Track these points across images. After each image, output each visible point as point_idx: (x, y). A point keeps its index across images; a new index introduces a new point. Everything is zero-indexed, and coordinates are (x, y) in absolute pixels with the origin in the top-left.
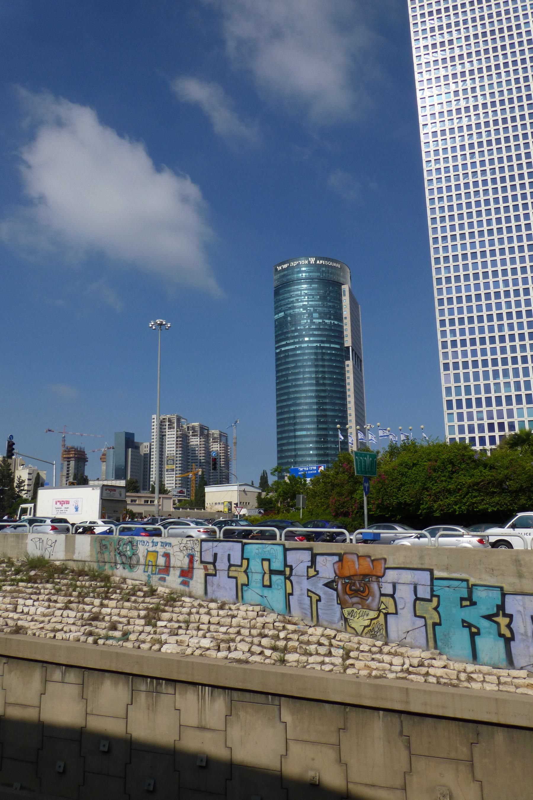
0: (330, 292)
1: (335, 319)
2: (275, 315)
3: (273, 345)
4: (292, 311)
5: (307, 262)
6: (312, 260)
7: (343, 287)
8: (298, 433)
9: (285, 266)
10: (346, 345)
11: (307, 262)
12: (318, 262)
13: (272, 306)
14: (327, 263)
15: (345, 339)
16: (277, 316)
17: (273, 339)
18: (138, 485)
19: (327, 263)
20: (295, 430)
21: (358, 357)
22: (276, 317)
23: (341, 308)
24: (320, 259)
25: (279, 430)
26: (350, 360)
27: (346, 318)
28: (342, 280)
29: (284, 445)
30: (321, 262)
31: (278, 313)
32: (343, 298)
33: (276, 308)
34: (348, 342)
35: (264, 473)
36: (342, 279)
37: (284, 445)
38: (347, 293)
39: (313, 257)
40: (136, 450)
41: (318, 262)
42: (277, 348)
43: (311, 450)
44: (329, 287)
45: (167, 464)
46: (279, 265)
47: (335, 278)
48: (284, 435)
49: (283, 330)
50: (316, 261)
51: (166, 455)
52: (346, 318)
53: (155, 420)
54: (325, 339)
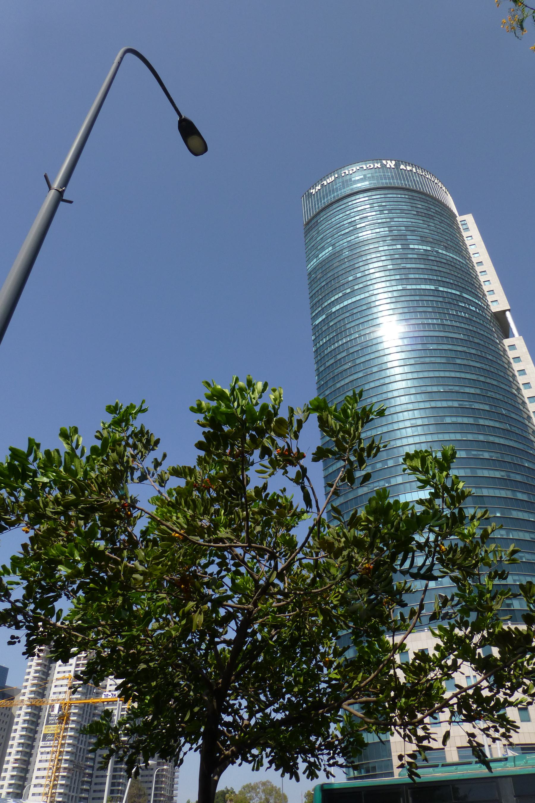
4: (353, 237)
6: (391, 164)
10: (495, 308)
12: (402, 167)
14: (419, 171)
15: (490, 298)
24: (406, 164)
30: (409, 168)
42: (314, 318)
45: (47, 723)
50: (397, 166)
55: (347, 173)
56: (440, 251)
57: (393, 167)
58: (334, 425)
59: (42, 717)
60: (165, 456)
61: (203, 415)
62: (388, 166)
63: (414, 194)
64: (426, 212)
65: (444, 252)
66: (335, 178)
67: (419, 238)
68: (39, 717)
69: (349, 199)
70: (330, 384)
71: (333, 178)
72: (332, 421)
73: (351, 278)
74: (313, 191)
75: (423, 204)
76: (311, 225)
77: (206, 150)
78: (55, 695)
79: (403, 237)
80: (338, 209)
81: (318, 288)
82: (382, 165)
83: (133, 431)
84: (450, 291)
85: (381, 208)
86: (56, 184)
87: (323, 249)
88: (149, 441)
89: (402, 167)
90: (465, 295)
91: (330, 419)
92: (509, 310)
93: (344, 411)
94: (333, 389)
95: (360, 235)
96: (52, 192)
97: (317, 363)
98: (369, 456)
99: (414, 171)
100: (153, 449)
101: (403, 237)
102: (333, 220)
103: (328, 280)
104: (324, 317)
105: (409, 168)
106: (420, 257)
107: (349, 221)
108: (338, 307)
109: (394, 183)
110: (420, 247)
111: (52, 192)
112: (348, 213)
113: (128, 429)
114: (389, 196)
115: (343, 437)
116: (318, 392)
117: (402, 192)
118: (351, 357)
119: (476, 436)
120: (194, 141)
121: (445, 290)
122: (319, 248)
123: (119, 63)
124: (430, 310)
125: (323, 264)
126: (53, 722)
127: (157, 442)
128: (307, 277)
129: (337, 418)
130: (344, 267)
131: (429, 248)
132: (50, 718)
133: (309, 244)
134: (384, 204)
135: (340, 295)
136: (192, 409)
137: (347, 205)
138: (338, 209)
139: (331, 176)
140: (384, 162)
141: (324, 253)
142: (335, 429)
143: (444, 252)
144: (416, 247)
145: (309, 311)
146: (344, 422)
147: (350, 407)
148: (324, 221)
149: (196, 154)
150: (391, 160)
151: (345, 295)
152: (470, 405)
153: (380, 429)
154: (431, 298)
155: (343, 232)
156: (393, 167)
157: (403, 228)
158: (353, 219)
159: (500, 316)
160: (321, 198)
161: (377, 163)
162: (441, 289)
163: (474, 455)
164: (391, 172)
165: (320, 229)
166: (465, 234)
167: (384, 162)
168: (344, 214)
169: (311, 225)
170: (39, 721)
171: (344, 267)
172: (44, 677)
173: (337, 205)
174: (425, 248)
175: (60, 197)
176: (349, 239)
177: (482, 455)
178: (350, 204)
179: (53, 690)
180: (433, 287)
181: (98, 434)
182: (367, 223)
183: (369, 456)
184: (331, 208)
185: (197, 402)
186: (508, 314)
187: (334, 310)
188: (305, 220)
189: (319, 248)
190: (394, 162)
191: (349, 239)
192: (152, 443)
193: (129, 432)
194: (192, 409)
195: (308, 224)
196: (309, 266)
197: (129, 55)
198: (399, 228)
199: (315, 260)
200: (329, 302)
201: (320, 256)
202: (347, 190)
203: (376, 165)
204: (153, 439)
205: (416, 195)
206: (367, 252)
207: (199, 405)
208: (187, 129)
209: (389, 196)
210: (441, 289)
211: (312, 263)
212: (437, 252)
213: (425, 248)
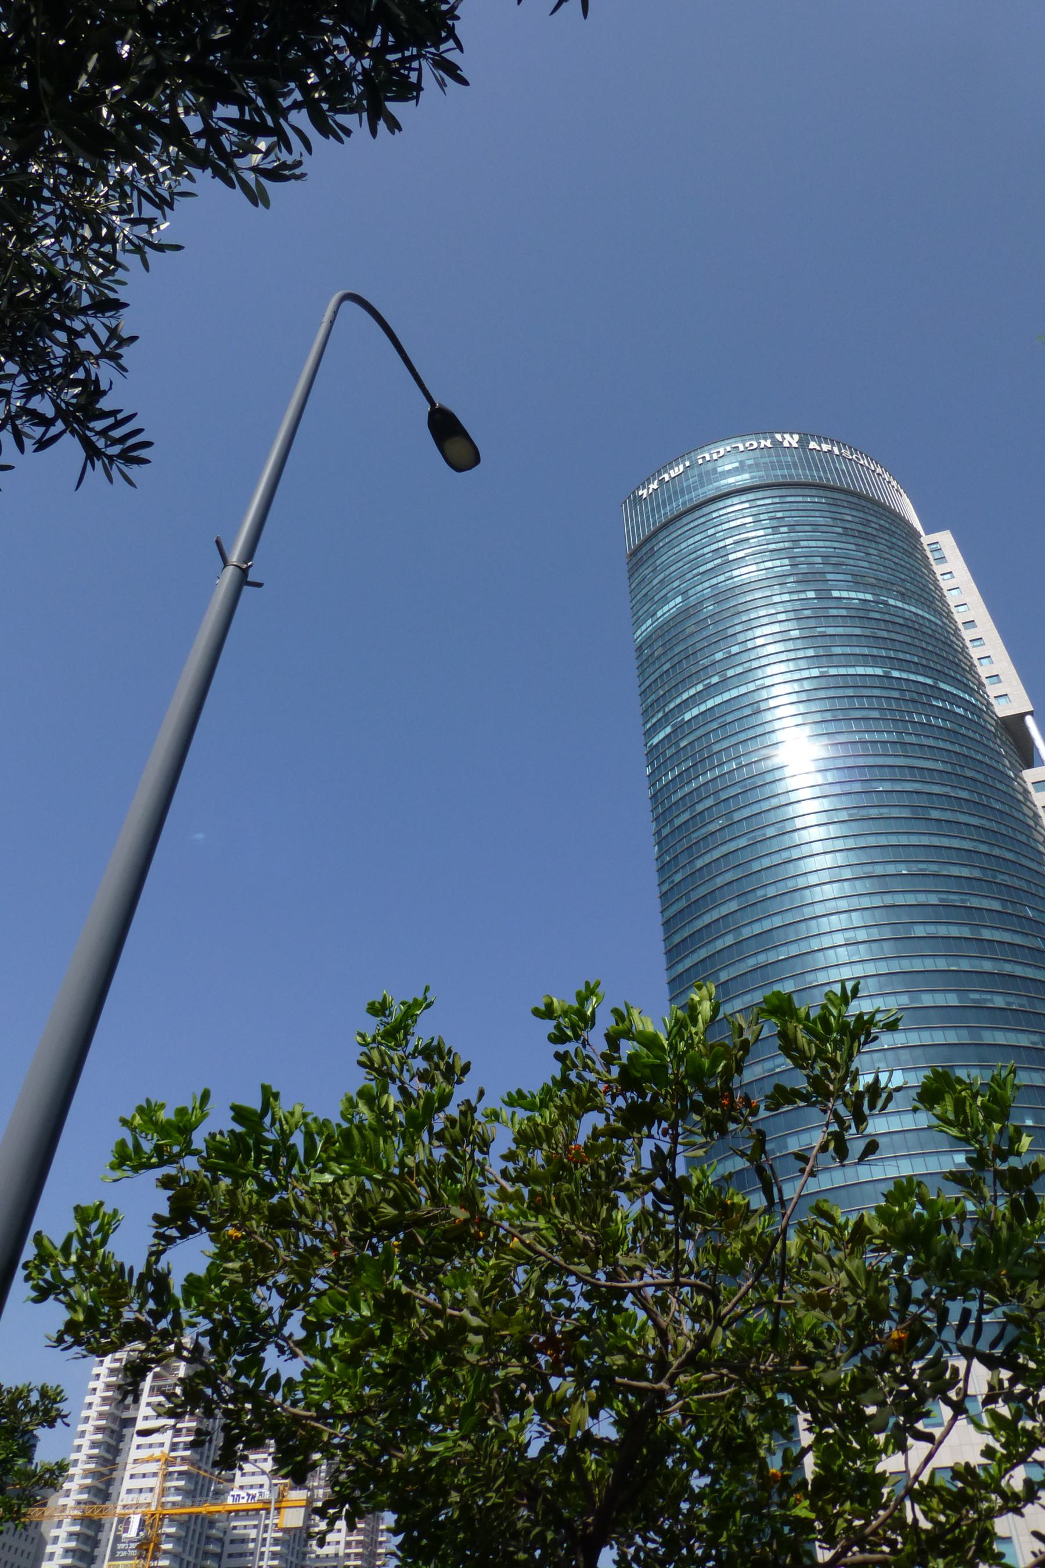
4: (722, 578)
5: (768, 443)
6: (791, 440)
10: (1003, 710)
11: (768, 443)
12: (813, 445)
14: (846, 453)
15: (992, 691)
24: (820, 439)
30: (826, 447)
42: (650, 733)
45: (113, 1557)
50: (803, 443)
51: (119, 1510)
55: (708, 458)
56: (891, 602)
57: (795, 445)
58: (806, 1048)
59: (103, 1543)
60: (482, 1093)
61: (555, 1023)
62: (786, 444)
63: (836, 495)
64: (861, 528)
65: (900, 604)
66: (686, 468)
67: (849, 578)
68: (95, 1543)
69: (713, 507)
70: (683, 860)
71: (681, 467)
72: (802, 1038)
73: (719, 656)
74: (643, 493)
75: (855, 513)
76: (641, 556)
77: (476, 460)
78: (131, 1496)
79: (818, 577)
80: (692, 525)
81: (656, 675)
82: (774, 442)
83: (416, 1047)
84: (912, 677)
85: (775, 523)
86: (235, 556)
87: (665, 600)
88: (450, 1068)
89: (813, 445)
90: (942, 685)
91: (800, 1034)
92: (1031, 713)
93: (824, 1019)
94: (688, 871)
95: (735, 573)
96: (230, 570)
97: (656, 819)
98: (872, 1107)
99: (836, 451)
100: (459, 1082)
101: (818, 577)
102: (683, 546)
103: (676, 660)
104: (668, 730)
105: (826, 447)
106: (853, 613)
107: (714, 547)
108: (695, 712)
109: (798, 475)
110: (853, 595)
111: (230, 570)
112: (710, 532)
113: (407, 1042)
114: (789, 499)
115: (824, 1070)
116: (660, 876)
117: (814, 492)
118: (723, 809)
119: (976, 962)
120: (456, 446)
121: (904, 675)
122: (656, 598)
123: (332, 322)
124: (875, 714)
125: (666, 628)
126: (124, 1554)
127: (466, 1069)
128: (635, 655)
129: (809, 1030)
130: (705, 634)
131: (869, 597)
132: (120, 1546)
133: (636, 591)
134: (779, 515)
135: (700, 687)
136: (536, 1012)
137: (709, 517)
138: (692, 525)
139: (678, 465)
140: (778, 437)
141: (666, 608)
142: (808, 1054)
143: (900, 604)
144: (845, 594)
145: (640, 720)
146: (824, 1041)
147: (835, 1012)
148: (666, 549)
149: (458, 468)
150: (791, 434)
151: (708, 687)
152: (962, 901)
153: (784, 949)
154: (877, 692)
155: (702, 569)
156: (795, 445)
157: (819, 560)
158: (721, 544)
159: (1014, 726)
160: (658, 506)
161: (765, 439)
162: (895, 674)
163: (973, 1001)
164: (792, 456)
165: (658, 562)
166: (938, 569)
167: (778, 437)
168: (703, 535)
169: (641, 556)
170: (97, 1552)
171: (705, 634)
172: (109, 1456)
173: (690, 518)
174: (861, 596)
175: (243, 579)
176: (714, 581)
177: (991, 1001)
178: (714, 515)
179: (127, 1484)
180: (879, 672)
181: (363, 1059)
182: (748, 550)
183: (872, 1107)
184: (678, 524)
185: (545, 1000)
186: (1029, 721)
187: (687, 716)
188: (629, 545)
189: (656, 598)
190: (796, 437)
191: (714, 581)
192: (458, 1071)
193: (410, 1049)
194: (536, 1012)
195: (634, 554)
196: (639, 633)
197: (348, 304)
198: (811, 560)
199: (649, 622)
200: (678, 701)
201: (659, 614)
202: (709, 490)
203: (763, 443)
204: (459, 1064)
205: (842, 497)
206: (750, 606)
207: (549, 1006)
208: (445, 427)
209: (789, 499)
210: (895, 674)
211: (644, 628)
212: (886, 603)
213: (861, 596)
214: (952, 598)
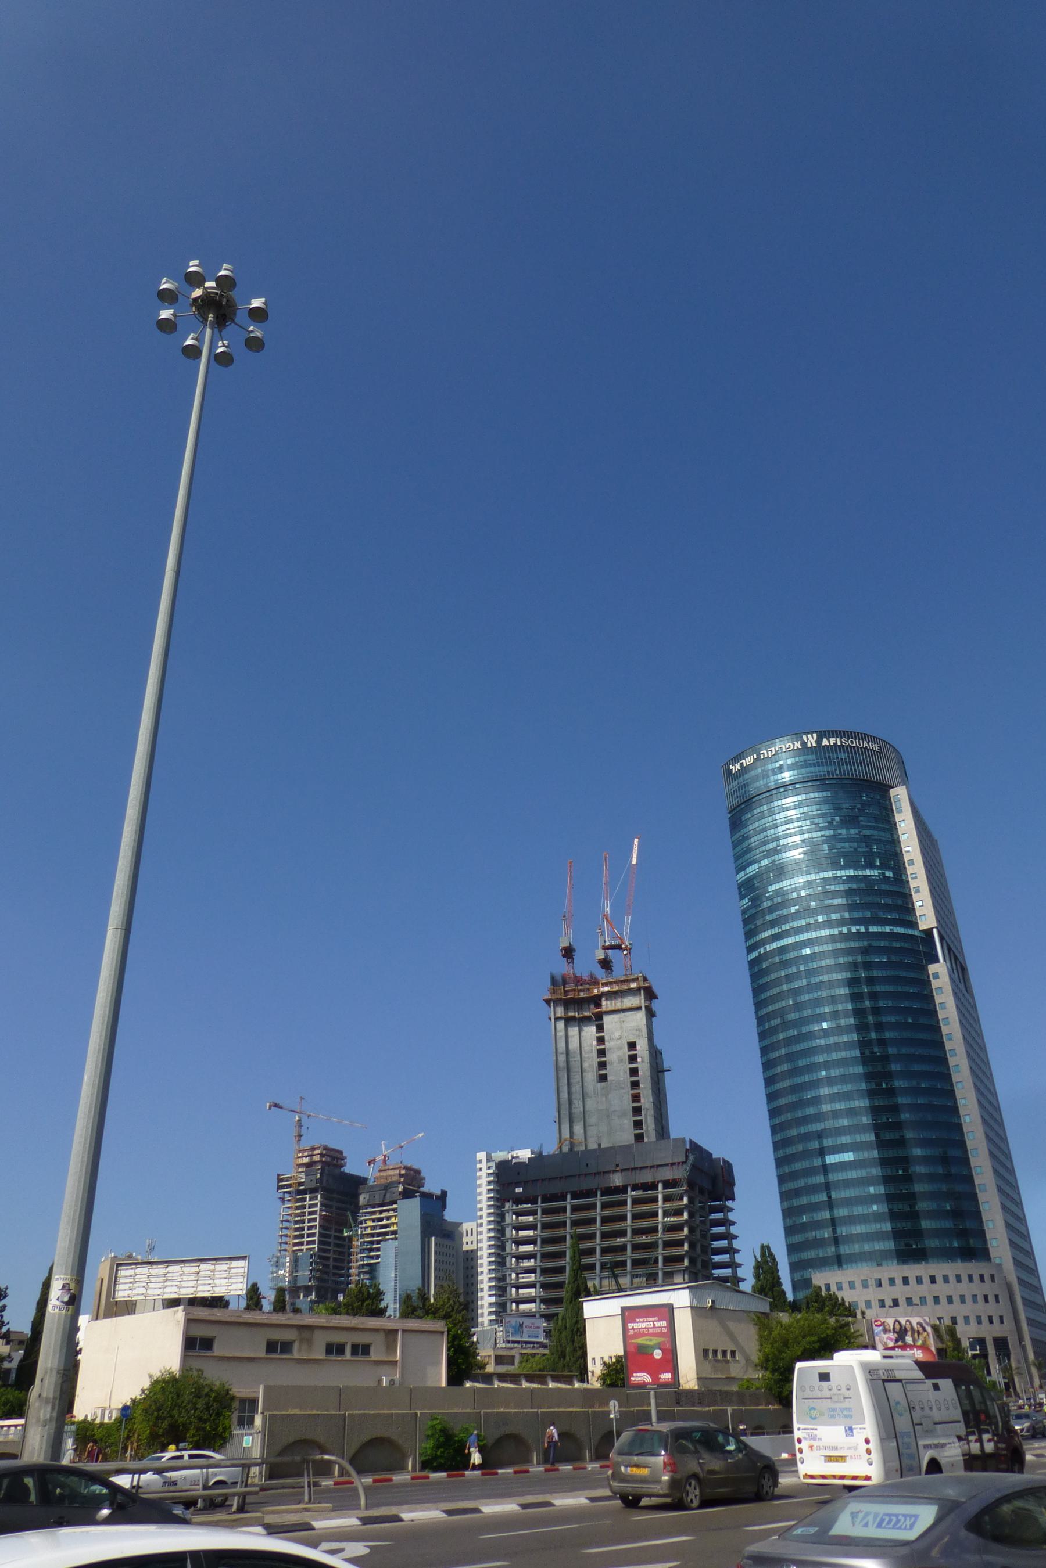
0: (864, 805)
1: (884, 866)
2: (738, 873)
3: (741, 944)
5: (798, 745)
7: (893, 792)
8: (830, 1159)
9: (748, 761)
10: (923, 926)
11: (798, 745)
12: (825, 742)
13: (729, 853)
14: (846, 742)
16: (742, 874)
17: (740, 931)
18: (383, 1305)
19: (846, 742)
20: (822, 1152)
21: (956, 958)
22: (741, 876)
23: (895, 842)
24: (829, 734)
25: (781, 1153)
26: (937, 961)
27: (911, 862)
28: (887, 778)
29: (797, 1193)
30: (832, 741)
31: (744, 868)
32: (898, 817)
33: (737, 857)
34: (926, 916)
35: (763, 1255)
36: (887, 776)
37: (797, 1193)
38: (906, 805)
39: (812, 733)
40: (447, 1242)
41: (825, 742)
42: (750, 949)
43: (873, 1203)
44: (856, 796)
46: (735, 760)
47: (871, 775)
48: (798, 1166)
49: (757, 910)
50: (819, 741)
52: (911, 862)
53: (484, 1165)
54: (868, 914)
57: (814, 745)
62: (809, 745)
156: (814, 745)
167: (804, 737)
186: (935, 930)
190: (815, 735)
214: (903, 838)
